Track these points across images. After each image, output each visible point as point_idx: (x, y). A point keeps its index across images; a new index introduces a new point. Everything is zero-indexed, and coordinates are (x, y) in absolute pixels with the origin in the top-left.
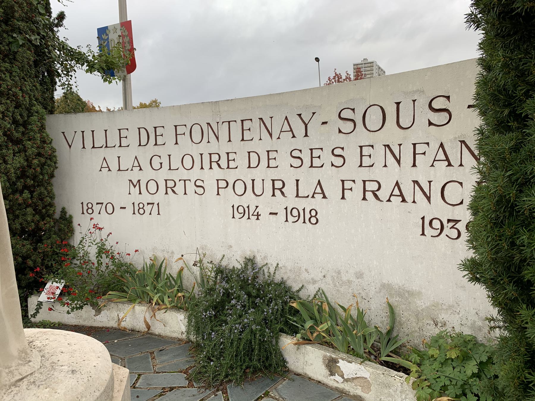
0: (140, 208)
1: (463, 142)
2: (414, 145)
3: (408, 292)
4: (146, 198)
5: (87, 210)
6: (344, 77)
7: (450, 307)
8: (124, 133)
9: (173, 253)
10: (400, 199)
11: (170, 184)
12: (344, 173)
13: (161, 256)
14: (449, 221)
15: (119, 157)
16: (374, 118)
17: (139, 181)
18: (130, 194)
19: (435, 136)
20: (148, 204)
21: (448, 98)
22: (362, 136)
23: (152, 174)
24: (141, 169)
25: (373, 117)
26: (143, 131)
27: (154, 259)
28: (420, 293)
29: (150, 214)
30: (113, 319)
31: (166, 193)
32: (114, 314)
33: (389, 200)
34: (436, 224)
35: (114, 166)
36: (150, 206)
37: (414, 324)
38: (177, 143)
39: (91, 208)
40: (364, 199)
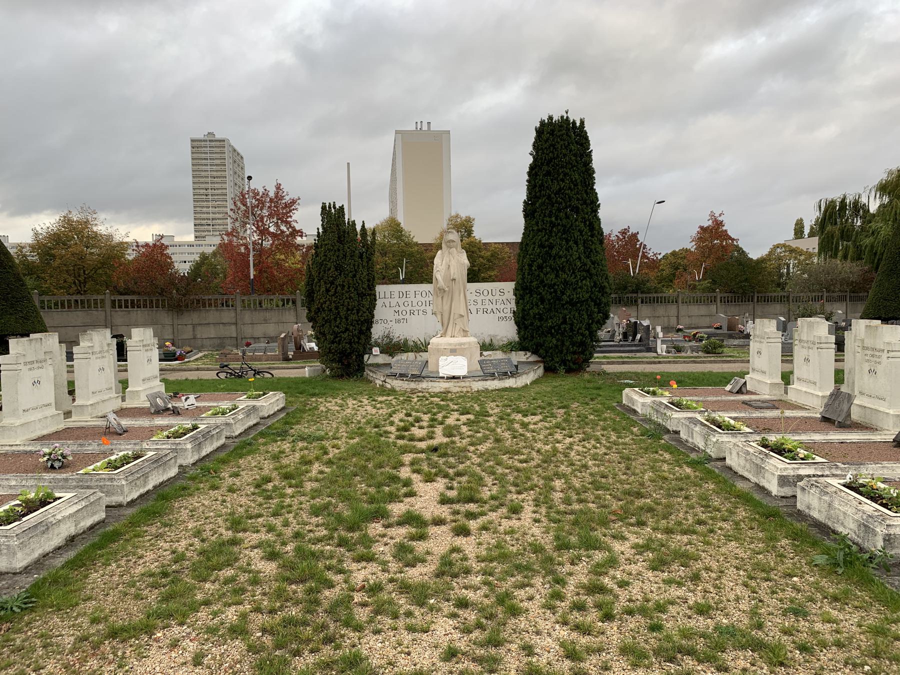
4: (401, 317)
6: (261, 194)
12: (477, 307)
16: (486, 293)
22: (482, 297)
23: (404, 308)
35: (388, 305)
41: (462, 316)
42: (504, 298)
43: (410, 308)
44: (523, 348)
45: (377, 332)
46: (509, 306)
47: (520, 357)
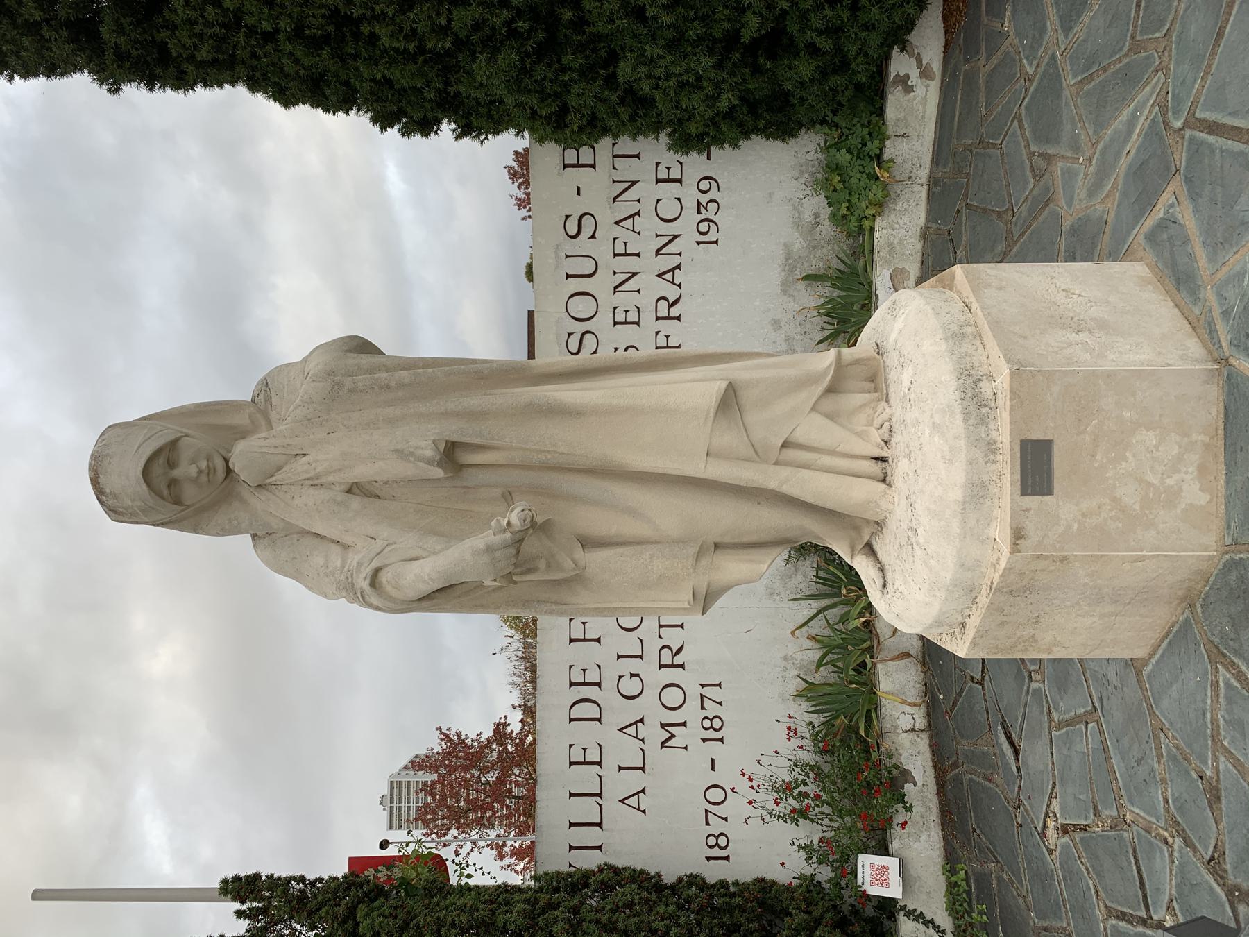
0: (711, 727)
1: (615, 200)
2: (615, 255)
3: (787, 260)
4: (691, 713)
5: (721, 848)
7: (795, 208)
8: (577, 756)
9: (785, 658)
10: (677, 271)
11: (666, 658)
13: (795, 685)
14: (699, 213)
15: (620, 768)
16: (582, 307)
17: (663, 726)
18: (686, 748)
19: (607, 230)
20: (703, 708)
21: (567, 217)
22: (602, 324)
23: (650, 696)
24: (641, 721)
25: (581, 307)
26: (578, 711)
27: (799, 695)
28: (785, 245)
29: (720, 703)
30: (913, 743)
31: (682, 666)
32: (904, 740)
33: (679, 286)
34: (704, 227)
35: (634, 781)
36: (707, 703)
37: (825, 250)
38: (598, 640)
39: (717, 838)
40: (678, 318)
41: (730, 401)
42: (606, 216)
43: (648, 669)
44: (872, 93)
45: (771, 851)
46: (646, 190)
47: (914, 110)
